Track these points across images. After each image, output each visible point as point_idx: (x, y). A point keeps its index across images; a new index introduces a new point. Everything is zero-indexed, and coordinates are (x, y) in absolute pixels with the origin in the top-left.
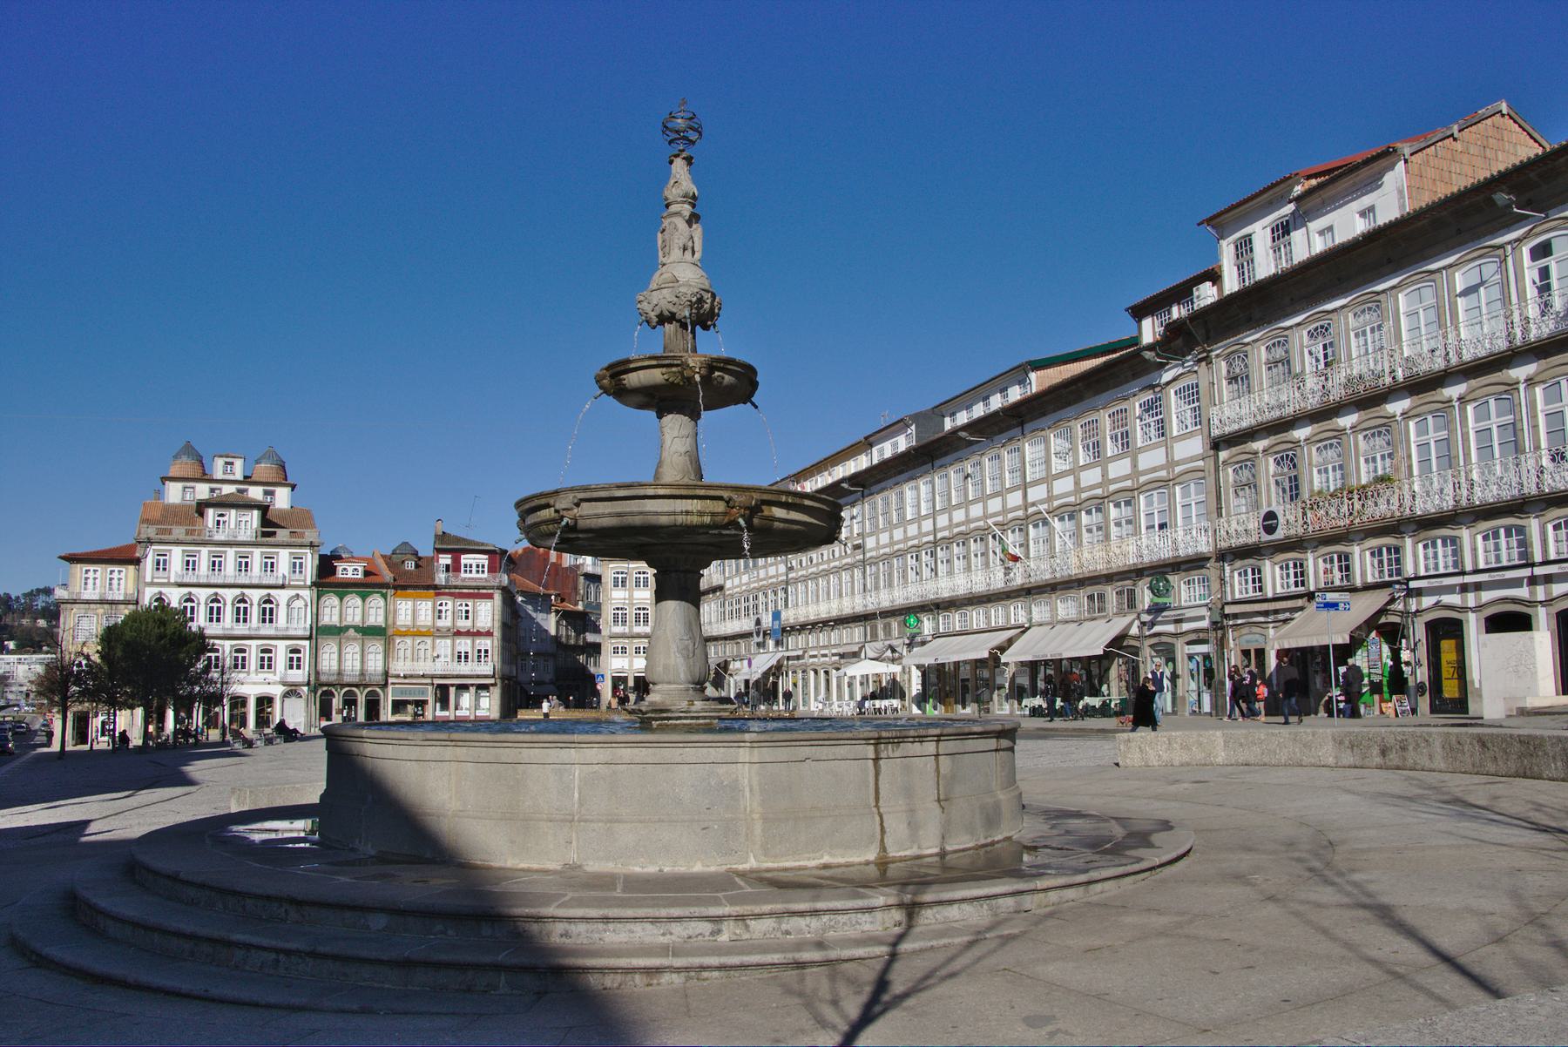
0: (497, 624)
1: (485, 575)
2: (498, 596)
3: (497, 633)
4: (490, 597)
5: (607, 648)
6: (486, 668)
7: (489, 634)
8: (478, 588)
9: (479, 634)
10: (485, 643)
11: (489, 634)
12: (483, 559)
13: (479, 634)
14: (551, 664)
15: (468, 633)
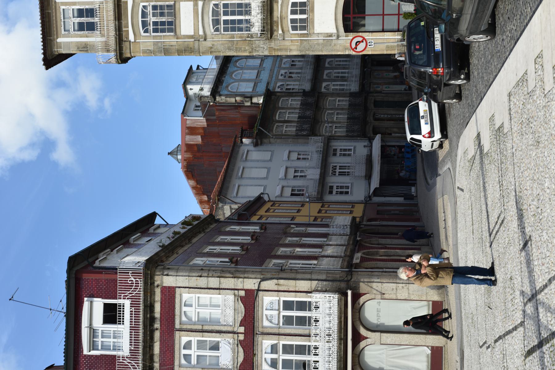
0: (229, 282)
1: (127, 303)
2: (169, 281)
3: (251, 284)
4: (169, 294)
5: (290, 43)
6: (326, 307)
7: (249, 300)
8: (149, 321)
9: (250, 320)
10: (270, 308)
11: (249, 300)
12: (94, 309)
13: (250, 320)
14: (339, 145)
15: (249, 345)
